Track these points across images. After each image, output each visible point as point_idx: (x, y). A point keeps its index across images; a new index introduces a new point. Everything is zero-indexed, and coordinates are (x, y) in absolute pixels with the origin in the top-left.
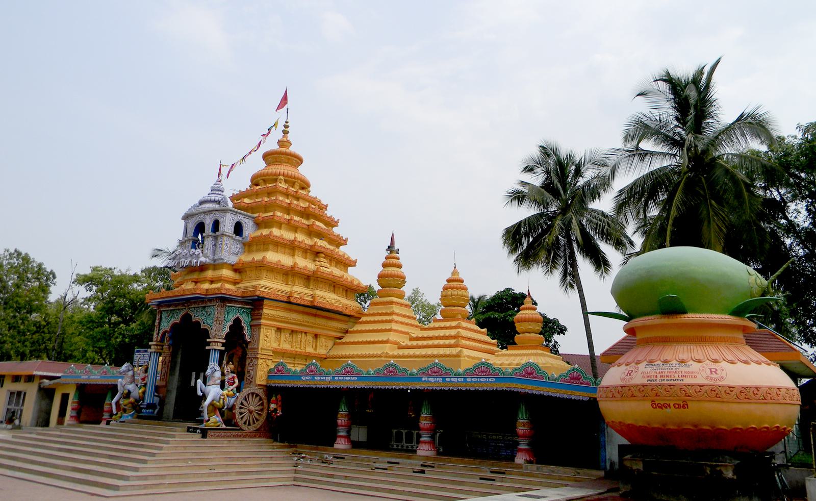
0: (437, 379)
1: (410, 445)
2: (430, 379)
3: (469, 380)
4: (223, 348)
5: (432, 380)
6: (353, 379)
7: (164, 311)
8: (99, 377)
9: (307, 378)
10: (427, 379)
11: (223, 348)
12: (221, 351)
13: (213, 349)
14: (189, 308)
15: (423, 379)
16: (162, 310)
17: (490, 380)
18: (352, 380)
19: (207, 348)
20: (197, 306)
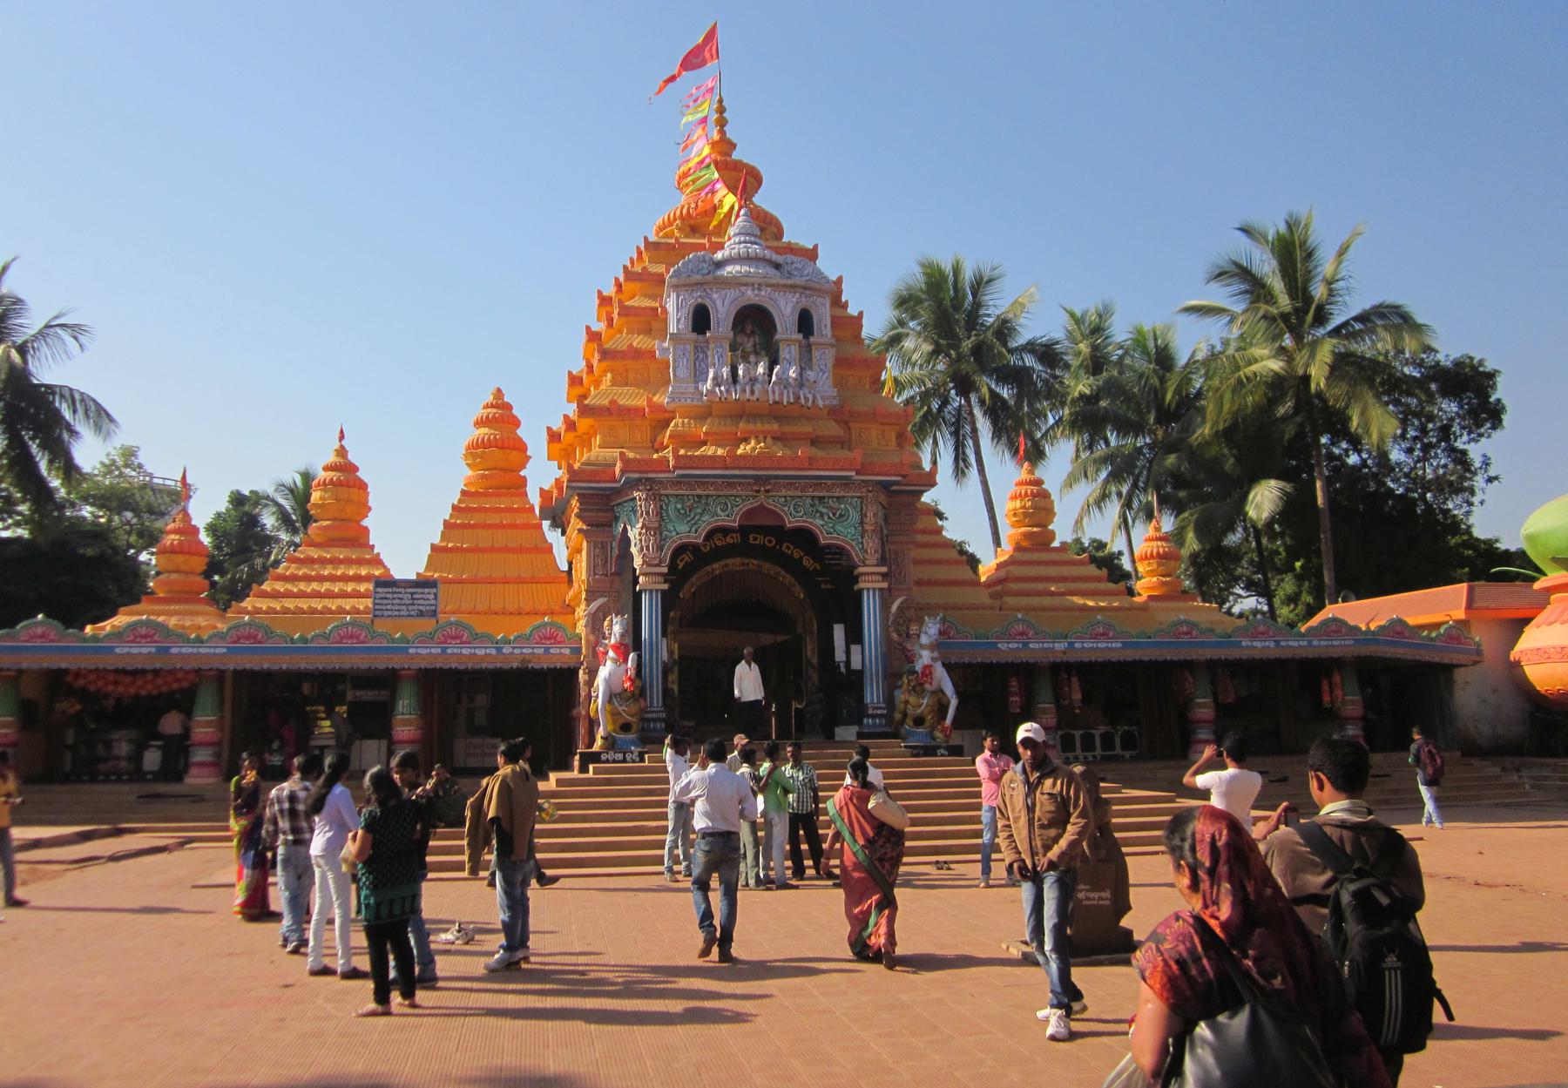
0: (1267, 643)
1: (1071, 755)
2: (1255, 644)
3: (1315, 643)
4: (885, 585)
5: (1258, 644)
6: (1114, 645)
7: (667, 496)
8: (224, 650)
9: (1010, 645)
10: (1249, 643)
11: (885, 585)
12: (881, 590)
13: (868, 589)
14: (768, 497)
15: (1244, 644)
16: (663, 492)
17: (1347, 642)
18: (1112, 648)
19: (861, 585)
20: (800, 494)
